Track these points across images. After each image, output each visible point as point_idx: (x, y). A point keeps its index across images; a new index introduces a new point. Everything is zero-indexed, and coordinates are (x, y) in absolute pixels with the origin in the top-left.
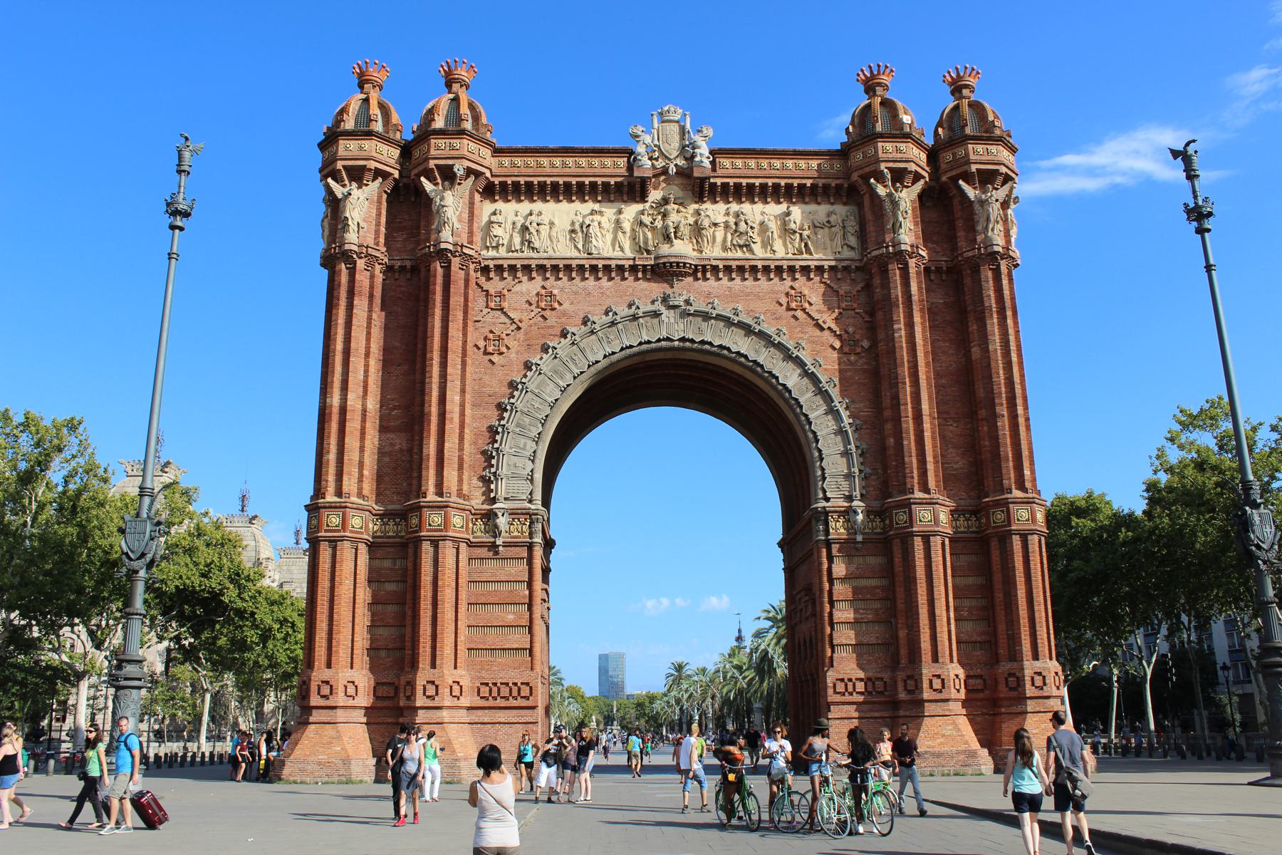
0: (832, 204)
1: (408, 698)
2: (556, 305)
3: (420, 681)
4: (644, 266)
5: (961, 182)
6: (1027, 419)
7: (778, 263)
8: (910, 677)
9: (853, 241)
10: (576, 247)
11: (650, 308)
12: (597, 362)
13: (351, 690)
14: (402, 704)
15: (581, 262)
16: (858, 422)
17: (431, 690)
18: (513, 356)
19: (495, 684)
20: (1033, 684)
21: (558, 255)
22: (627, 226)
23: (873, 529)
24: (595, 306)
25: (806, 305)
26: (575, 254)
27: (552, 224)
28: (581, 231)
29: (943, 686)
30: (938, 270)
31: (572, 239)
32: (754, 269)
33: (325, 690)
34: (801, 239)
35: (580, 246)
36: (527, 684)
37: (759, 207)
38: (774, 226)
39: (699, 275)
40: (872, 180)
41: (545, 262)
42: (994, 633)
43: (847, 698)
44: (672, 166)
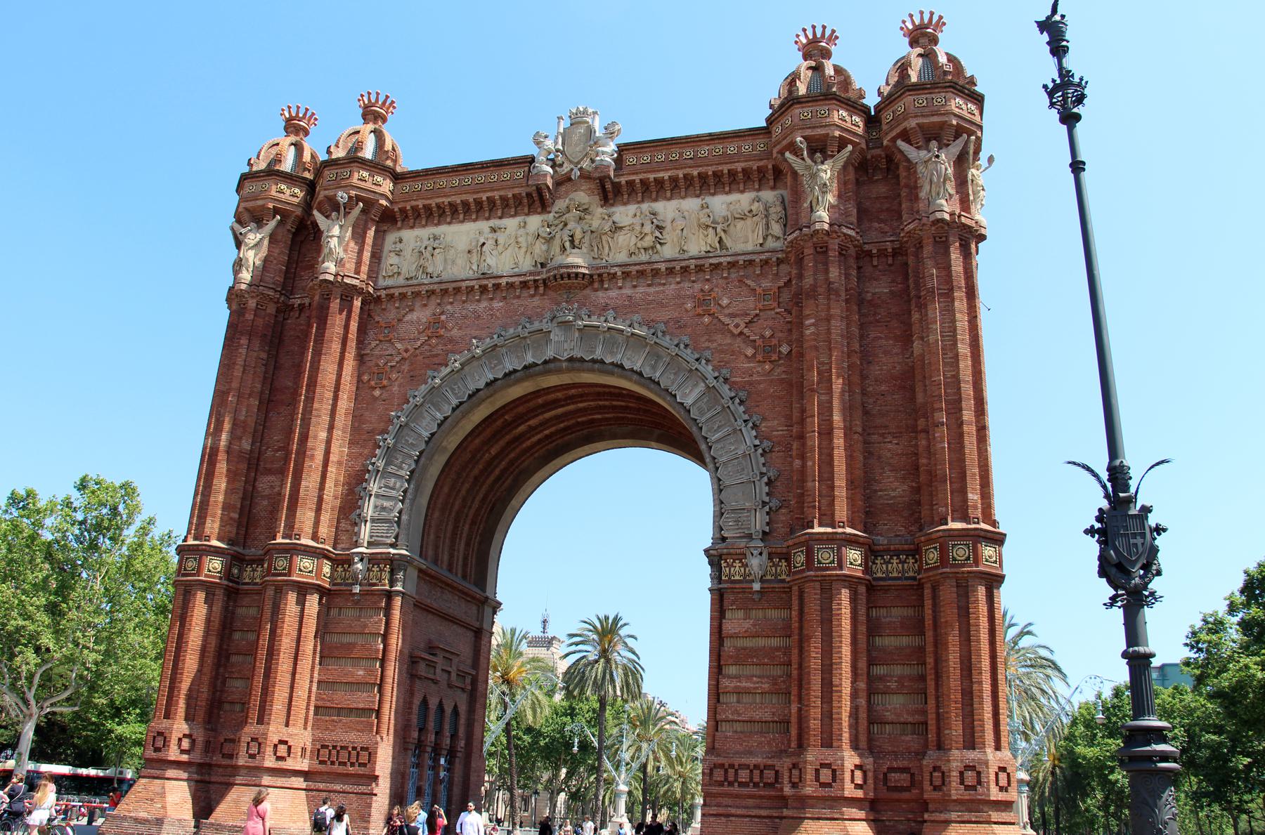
0: (759, 190)
2: (442, 332)
3: (245, 739)
4: (535, 281)
5: (900, 143)
6: (982, 430)
7: (684, 264)
8: (795, 766)
9: (776, 229)
11: (537, 325)
12: (478, 390)
13: (186, 744)
15: (472, 283)
16: (766, 444)
18: (395, 389)
19: (335, 747)
20: (962, 783)
23: (776, 574)
24: (483, 329)
25: (713, 308)
26: (470, 274)
27: (447, 248)
29: (834, 780)
32: (656, 273)
33: (160, 743)
36: (366, 749)
40: (787, 154)
41: (436, 287)
42: (924, 712)
44: (576, 170)
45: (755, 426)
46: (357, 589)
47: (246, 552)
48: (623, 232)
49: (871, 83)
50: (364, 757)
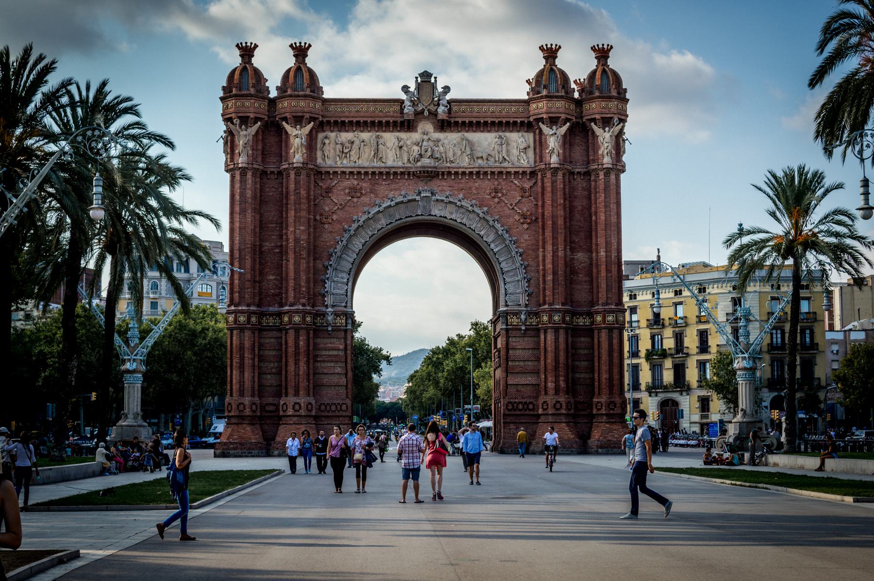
1: (284, 411)
13: (254, 407)
14: (281, 413)
17: (297, 407)
25: (500, 195)
30: (578, 173)
43: (513, 412)
45: (521, 255)
46: (330, 329)
47: (264, 309)
50: (344, 407)
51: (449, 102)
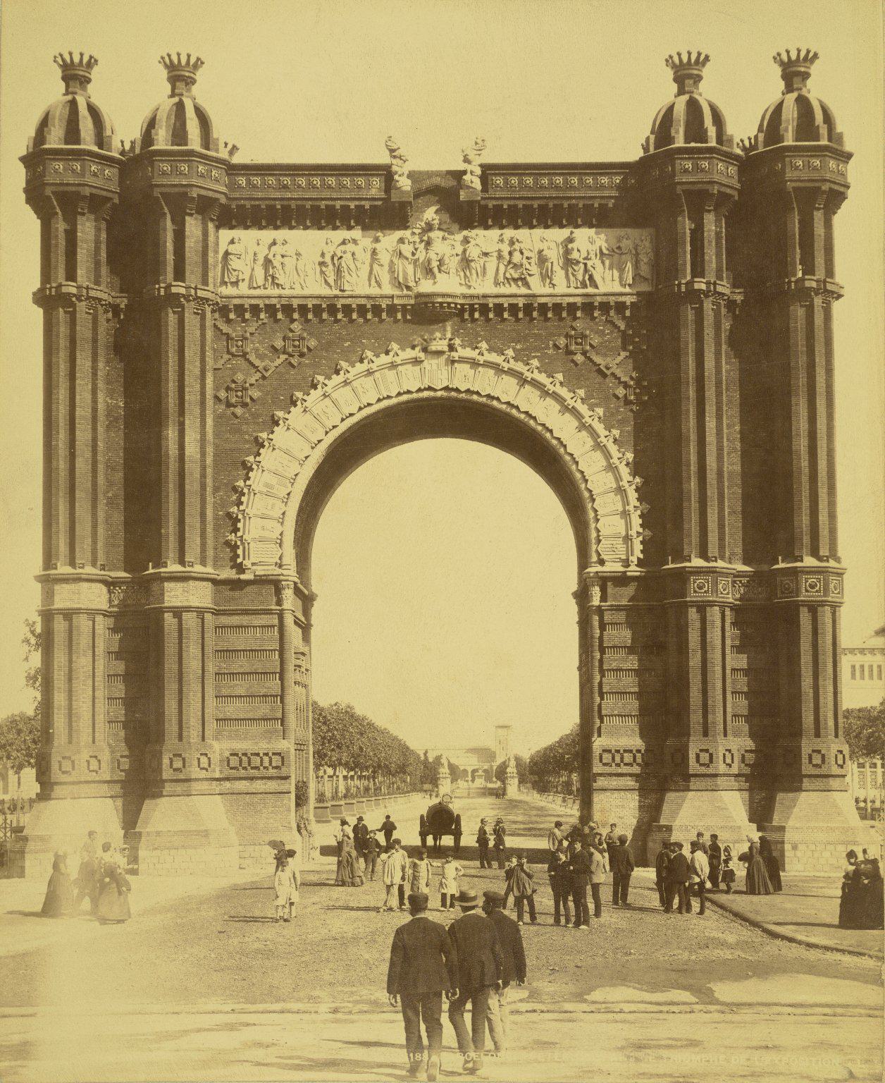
4: (404, 306)
10: (326, 281)
21: (306, 292)
22: (385, 258)
26: (326, 291)
27: (298, 254)
28: (334, 265)
31: (322, 272)
34: (586, 270)
35: (331, 281)
37: (538, 232)
38: (554, 255)
39: (466, 316)
48: (490, 259)
49: (743, 127)
51: (485, 167)
